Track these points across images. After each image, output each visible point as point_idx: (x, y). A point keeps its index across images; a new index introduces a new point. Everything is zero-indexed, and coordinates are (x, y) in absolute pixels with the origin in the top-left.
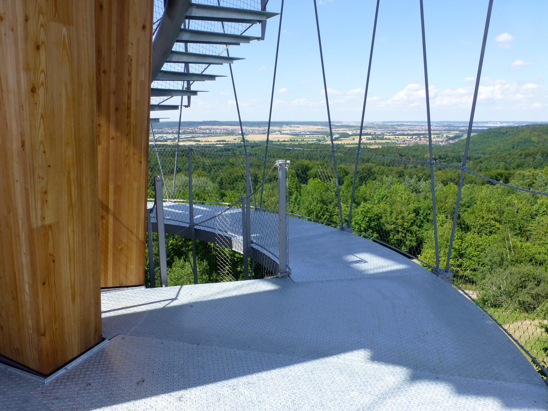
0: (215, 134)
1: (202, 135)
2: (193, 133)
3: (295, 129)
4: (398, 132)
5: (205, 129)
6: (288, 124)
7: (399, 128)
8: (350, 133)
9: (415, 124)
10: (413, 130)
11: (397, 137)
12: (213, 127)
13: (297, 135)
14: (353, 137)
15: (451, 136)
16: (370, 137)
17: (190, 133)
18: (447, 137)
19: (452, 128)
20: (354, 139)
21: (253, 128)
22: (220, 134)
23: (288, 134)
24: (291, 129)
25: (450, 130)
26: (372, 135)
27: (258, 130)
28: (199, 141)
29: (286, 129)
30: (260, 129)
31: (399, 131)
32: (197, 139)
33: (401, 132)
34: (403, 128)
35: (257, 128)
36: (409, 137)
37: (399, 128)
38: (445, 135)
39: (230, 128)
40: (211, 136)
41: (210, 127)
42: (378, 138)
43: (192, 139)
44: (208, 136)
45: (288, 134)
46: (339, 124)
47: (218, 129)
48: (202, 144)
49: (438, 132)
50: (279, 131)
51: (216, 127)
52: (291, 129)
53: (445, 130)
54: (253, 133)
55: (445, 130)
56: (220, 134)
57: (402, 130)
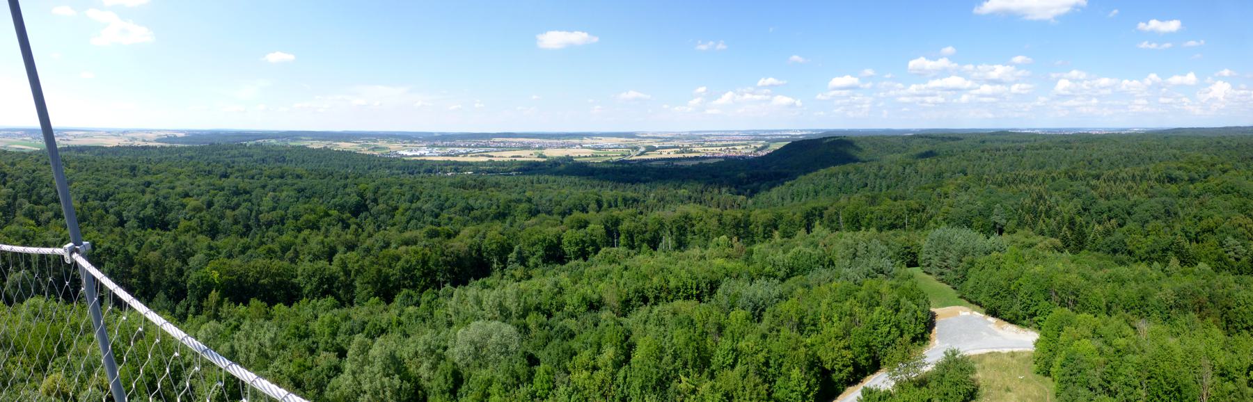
0: (510, 148)
1: (495, 149)
2: (486, 147)
3: (598, 141)
4: (706, 143)
5: (499, 142)
6: (589, 135)
7: (707, 138)
8: (657, 147)
9: (723, 133)
10: (721, 141)
11: (706, 148)
12: (507, 139)
13: (599, 149)
14: (660, 150)
15: (759, 146)
16: (679, 149)
17: (483, 146)
18: (755, 147)
19: (758, 137)
20: (661, 154)
21: (552, 141)
22: (515, 147)
23: (589, 148)
24: (593, 141)
25: (757, 140)
26: (680, 148)
27: (557, 143)
28: (493, 156)
29: (587, 141)
30: (558, 142)
31: (707, 142)
32: (490, 154)
33: (709, 143)
34: (711, 138)
35: (555, 141)
36: (719, 148)
37: (707, 138)
38: (753, 146)
39: (526, 140)
40: (506, 151)
41: (504, 139)
42: (686, 151)
43: (485, 154)
44: (503, 151)
45: (589, 148)
46: (645, 136)
47: (513, 142)
48: (496, 159)
49: (746, 142)
50: (580, 145)
51: (511, 140)
52: (593, 141)
53: (752, 140)
54: (551, 147)
55: (752, 140)
56: (515, 147)
57: (711, 141)
